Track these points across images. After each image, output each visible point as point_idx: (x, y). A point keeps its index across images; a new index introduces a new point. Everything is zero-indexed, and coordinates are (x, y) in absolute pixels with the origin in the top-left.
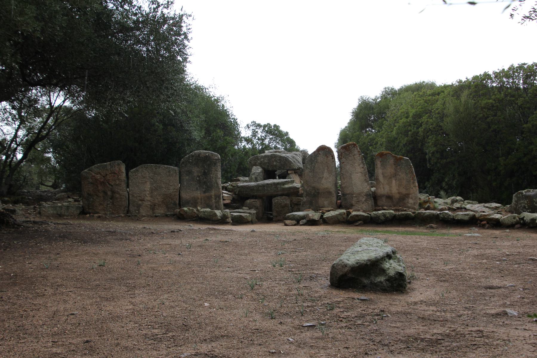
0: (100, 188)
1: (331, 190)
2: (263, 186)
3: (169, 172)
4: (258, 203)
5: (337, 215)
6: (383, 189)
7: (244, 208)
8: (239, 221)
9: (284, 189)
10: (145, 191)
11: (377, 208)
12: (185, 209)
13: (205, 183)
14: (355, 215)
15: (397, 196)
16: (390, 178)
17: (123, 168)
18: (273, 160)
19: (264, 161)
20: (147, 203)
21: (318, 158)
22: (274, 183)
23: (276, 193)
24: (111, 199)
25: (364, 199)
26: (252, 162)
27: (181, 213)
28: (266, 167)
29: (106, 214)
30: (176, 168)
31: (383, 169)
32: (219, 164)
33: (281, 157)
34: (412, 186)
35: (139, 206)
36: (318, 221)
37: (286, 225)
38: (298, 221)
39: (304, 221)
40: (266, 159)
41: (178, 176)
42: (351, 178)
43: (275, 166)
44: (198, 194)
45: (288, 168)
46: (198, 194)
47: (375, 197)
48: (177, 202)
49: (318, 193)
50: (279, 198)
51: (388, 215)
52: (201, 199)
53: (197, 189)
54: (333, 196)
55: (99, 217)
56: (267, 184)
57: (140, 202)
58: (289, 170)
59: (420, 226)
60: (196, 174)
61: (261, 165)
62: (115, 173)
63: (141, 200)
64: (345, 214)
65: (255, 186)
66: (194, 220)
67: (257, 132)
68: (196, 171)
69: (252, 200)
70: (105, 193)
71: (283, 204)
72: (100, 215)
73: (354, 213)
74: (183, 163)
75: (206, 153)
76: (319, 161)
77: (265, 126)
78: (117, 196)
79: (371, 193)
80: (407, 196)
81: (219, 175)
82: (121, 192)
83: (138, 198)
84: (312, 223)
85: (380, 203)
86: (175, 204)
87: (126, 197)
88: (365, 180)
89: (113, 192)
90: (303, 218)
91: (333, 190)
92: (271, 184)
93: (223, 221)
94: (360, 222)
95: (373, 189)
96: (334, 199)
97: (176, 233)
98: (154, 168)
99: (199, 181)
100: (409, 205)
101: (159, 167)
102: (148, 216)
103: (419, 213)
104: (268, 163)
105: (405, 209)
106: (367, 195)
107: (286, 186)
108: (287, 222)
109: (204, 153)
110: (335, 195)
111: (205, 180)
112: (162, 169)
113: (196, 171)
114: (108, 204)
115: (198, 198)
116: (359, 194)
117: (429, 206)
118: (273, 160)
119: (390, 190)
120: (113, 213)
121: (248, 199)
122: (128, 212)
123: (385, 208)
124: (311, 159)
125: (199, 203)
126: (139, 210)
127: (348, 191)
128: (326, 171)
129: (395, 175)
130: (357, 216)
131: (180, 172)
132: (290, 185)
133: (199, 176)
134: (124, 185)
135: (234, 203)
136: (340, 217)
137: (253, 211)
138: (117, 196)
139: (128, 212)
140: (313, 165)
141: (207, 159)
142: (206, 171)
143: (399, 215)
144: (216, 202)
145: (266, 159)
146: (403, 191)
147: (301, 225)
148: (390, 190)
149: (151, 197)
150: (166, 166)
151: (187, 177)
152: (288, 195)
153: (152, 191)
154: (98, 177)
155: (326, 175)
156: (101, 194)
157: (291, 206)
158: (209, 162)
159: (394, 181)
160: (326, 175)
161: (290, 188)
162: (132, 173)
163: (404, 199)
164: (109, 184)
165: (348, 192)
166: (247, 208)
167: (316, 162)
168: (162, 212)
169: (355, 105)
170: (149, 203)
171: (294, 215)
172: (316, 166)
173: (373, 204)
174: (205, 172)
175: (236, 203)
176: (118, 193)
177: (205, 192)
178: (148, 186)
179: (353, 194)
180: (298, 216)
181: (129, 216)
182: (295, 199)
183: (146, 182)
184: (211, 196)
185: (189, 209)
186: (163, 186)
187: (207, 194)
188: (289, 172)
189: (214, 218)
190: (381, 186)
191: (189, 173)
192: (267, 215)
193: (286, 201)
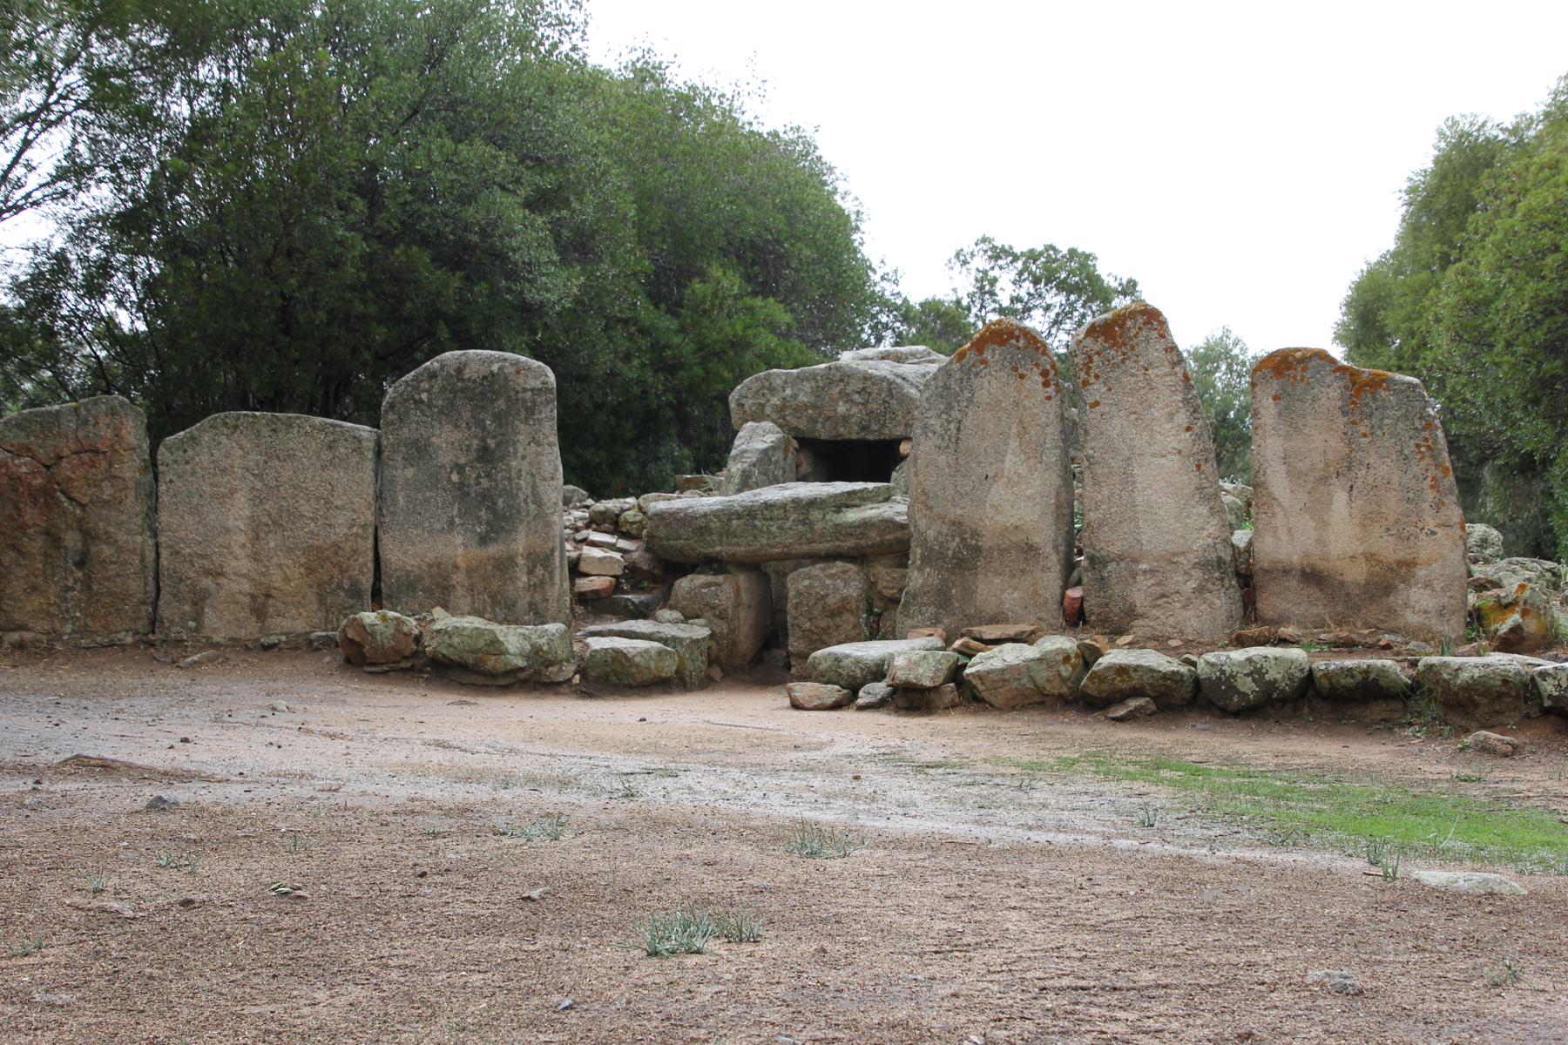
0: (30, 515)
1: (1036, 539)
2: (750, 513)
3: (331, 447)
4: (727, 590)
5: (1025, 668)
6: (1284, 539)
7: (666, 614)
8: (611, 680)
9: (840, 530)
10: (228, 531)
11: (1253, 630)
12: (369, 617)
13: (486, 497)
14: (1108, 668)
15: (1356, 573)
16: (1324, 480)
17: (134, 431)
18: (835, 390)
19: (794, 396)
20: (235, 587)
21: (976, 382)
22: (796, 502)
23: (805, 548)
24: (80, 564)
25: (1192, 584)
26: (748, 403)
27: (351, 634)
28: (802, 424)
29: (55, 635)
30: (365, 431)
31: (1287, 437)
32: (549, 416)
33: (867, 378)
34: (1431, 523)
35: (199, 599)
36: (935, 689)
37: (796, 706)
38: (849, 690)
39: (880, 689)
40: (807, 386)
41: (370, 465)
42: (1128, 478)
43: (846, 419)
44: (458, 548)
46: (458, 548)
47: (1244, 577)
48: (367, 582)
49: (977, 550)
50: (816, 569)
51: (1273, 674)
52: (470, 571)
53: (451, 523)
54: (1045, 569)
55: (20, 646)
56: (768, 506)
57: (206, 582)
59: (1433, 735)
60: (446, 458)
62: (97, 452)
63: (208, 573)
64: (1067, 659)
65: (716, 514)
66: (405, 670)
67: (994, 281)
68: (448, 442)
69: (701, 579)
70: (55, 540)
71: (832, 601)
72: (28, 636)
73: (1114, 656)
74: (392, 406)
75: (491, 361)
76: (982, 396)
77: (1032, 256)
78: (107, 551)
79: (1227, 555)
80: (1404, 569)
81: (552, 460)
82: (122, 537)
83: (199, 563)
84: (911, 699)
85: (1269, 604)
86: (355, 593)
87: (143, 559)
88: (1200, 489)
89: (88, 535)
90: (878, 672)
91: (1045, 535)
92: (782, 506)
93: (532, 679)
94: (1133, 704)
95: (1240, 538)
96: (1051, 579)
98: (265, 432)
99: (461, 490)
100: (1412, 618)
101: (290, 426)
102: (234, 642)
103: (1431, 667)
104: (814, 407)
105: (1386, 638)
106: (1203, 565)
107: (852, 516)
108: (803, 690)
109: (483, 361)
110: (1054, 561)
111: (485, 483)
112: (306, 433)
113: (448, 442)
114: (68, 589)
115: (456, 567)
116: (1171, 559)
117: (1516, 629)
118: (835, 390)
119: (1320, 541)
120: (84, 631)
122: (154, 622)
123: (1288, 631)
124: (946, 387)
125: (460, 591)
126: (198, 617)
127: (1111, 543)
128: (1014, 444)
129: (1348, 465)
130: (1122, 670)
131: (379, 452)
132: (870, 512)
133: (460, 469)
134: (133, 505)
135: (636, 588)
136: (1042, 675)
137: (699, 631)
138: (107, 551)
139: (154, 622)
140: (955, 414)
141: (491, 387)
142: (491, 442)
143: (1327, 675)
144: (530, 587)
145: (807, 386)
146: (1389, 549)
147: (862, 708)
148: (1320, 541)
149: (255, 557)
150: (318, 420)
151: (410, 473)
152: (859, 557)
153: (257, 531)
154: (23, 466)
155: (1012, 462)
156: (36, 545)
157: (870, 611)
158: (501, 404)
159: (1340, 497)
160: (1012, 462)
161: (866, 524)
162: (170, 449)
163: (1388, 589)
164: (71, 499)
165: (1115, 549)
166: (676, 615)
167: (970, 400)
168: (300, 626)
169: (1420, 156)
170: (246, 587)
171: (838, 659)
172: (967, 422)
173: (1237, 609)
175: (643, 590)
176: (109, 540)
177: (484, 540)
178: (239, 513)
179: (1136, 561)
180: (858, 661)
181: (152, 644)
183: (233, 492)
184: (512, 559)
185: (384, 618)
186: (306, 509)
187: (493, 550)
189: (491, 663)
190: (1279, 521)
191: (419, 451)
192: (761, 655)
193: (844, 583)
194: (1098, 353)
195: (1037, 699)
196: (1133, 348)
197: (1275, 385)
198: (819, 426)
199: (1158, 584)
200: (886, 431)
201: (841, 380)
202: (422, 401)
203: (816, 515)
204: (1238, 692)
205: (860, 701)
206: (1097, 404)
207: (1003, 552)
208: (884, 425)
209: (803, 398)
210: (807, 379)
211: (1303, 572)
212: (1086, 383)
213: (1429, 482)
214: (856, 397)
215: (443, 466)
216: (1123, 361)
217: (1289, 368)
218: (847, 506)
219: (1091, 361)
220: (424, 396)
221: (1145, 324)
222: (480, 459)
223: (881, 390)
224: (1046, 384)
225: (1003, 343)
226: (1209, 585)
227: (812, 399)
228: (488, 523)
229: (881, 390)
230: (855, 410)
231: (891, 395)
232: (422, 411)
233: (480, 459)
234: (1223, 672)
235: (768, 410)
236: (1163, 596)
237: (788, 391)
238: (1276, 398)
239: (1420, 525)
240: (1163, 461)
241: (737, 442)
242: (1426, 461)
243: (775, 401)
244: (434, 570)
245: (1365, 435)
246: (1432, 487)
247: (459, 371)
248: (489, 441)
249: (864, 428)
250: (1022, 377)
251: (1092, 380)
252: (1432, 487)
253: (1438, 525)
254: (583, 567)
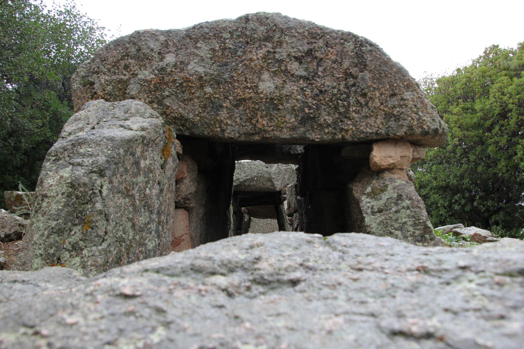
18: (257, 55)
19: (181, 66)
28: (192, 112)
43: (274, 103)
61: (154, 94)
104: (217, 82)
118: (257, 55)
188: (380, 155)
198: (223, 114)
200: (348, 125)
201: (268, 39)
208: (346, 115)
209: (195, 68)
210: (205, 37)
214: (294, 66)
223: (342, 54)
227: (213, 70)
229: (342, 54)
230: (291, 87)
231: (363, 65)
235: (133, 88)
237: (170, 59)
241: (68, 128)
243: (145, 74)
249: (306, 120)
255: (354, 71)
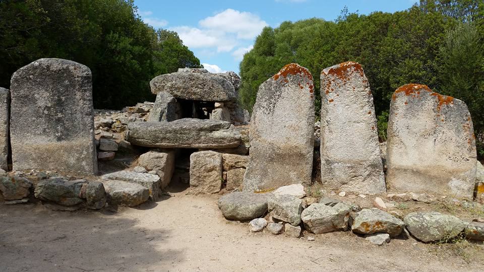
1: (304, 152)
21: (283, 89)
25: (367, 173)
28: (179, 94)
45: (216, 98)
54: (307, 163)
58: (217, 102)
60: (41, 103)
68: (43, 98)
71: (208, 166)
74: (16, 80)
97: (41, 177)
111: (60, 115)
113: (43, 98)
121: (145, 149)
133: (47, 108)
142: (63, 98)
172: (278, 104)
174: (60, 100)
182: (229, 158)
188: (217, 105)
193: (213, 159)
194: (333, 81)
195: (332, 230)
196: (349, 79)
197: (405, 99)
199: (354, 172)
202: (30, 79)
203: (202, 133)
204: (429, 234)
205: (254, 229)
206: (332, 100)
207: (290, 156)
211: (413, 171)
212: (328, 92)
213: (468, 140)
215: (40, 107)
216: (344, 84)
217: (412, 92)
218: (214, 130)
219: (330, 83)
220: (31, 76)
221: (355, 70)
222: (57, 104)
224: (311, 91)
225: (295, 73)
226: (374, 173)
228: (61, 132)
232: (30, 83)
233: (57, 104)
234: (423, 225)
235: (166, 88)
236: (355, 176)
238: (406, 103)
239: (463, 157)
240: (358, 124)
242: (467, 132)
244: (37, 151)
245: (443, 121)
246: (469, 143)
247: (48, 67)
248: (61, 97)
250: (302, 88)
251: (330, 91)
252: (469, 143)
253: (470, 157)
254: (102, 148)
255: (212, 87)
